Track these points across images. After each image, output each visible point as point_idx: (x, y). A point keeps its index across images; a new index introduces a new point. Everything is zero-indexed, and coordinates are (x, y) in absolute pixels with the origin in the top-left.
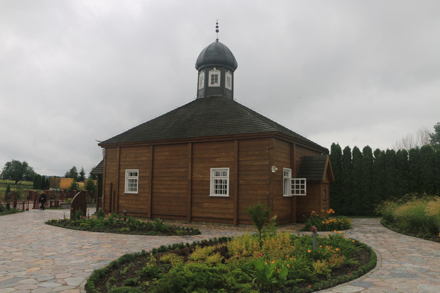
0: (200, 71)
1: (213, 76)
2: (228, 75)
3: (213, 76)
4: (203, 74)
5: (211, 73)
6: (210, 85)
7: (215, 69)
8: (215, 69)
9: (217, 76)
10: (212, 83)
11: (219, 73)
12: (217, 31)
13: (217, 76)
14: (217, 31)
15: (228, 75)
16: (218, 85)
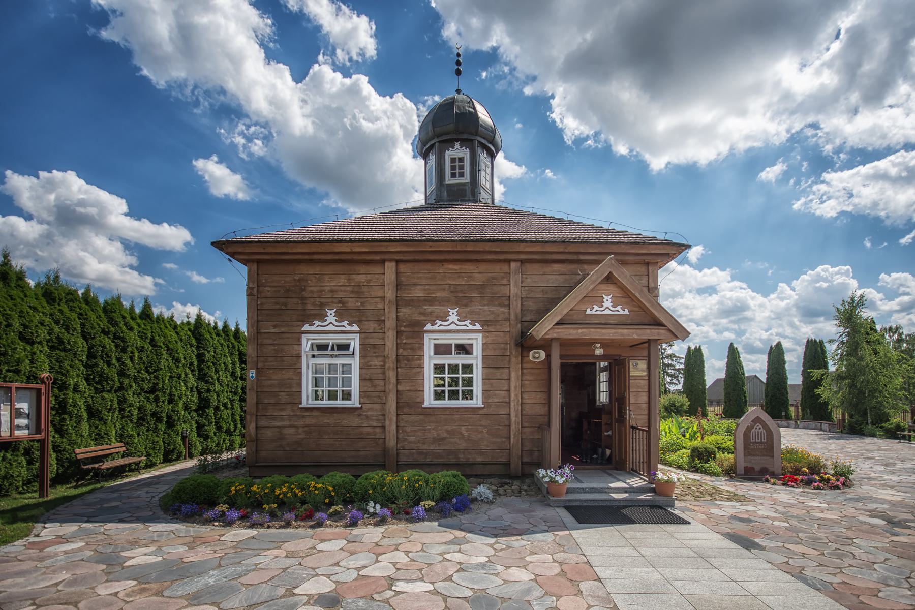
0: (425, 156)
1: (453, 160)
2: (483, 157)
3: (453, 160)
4: (432, 158)
5: (450, 154)
6: (449, 180)
7: (457, 145)
8: (457, 145)
9: (461, 160)
10: (453, 175)
11: (465, 153)
12: (458, 72)
13: (461, 160)
14: (458, 72)
15: (483, 157)
16: (467, 179)
